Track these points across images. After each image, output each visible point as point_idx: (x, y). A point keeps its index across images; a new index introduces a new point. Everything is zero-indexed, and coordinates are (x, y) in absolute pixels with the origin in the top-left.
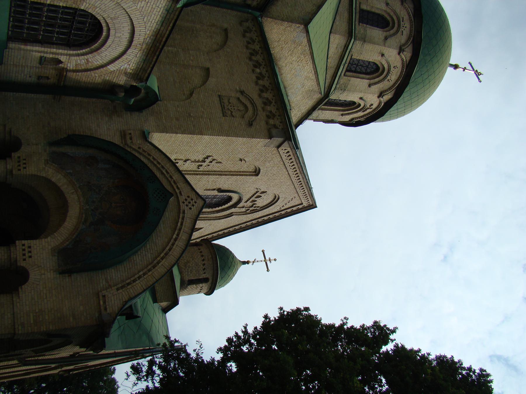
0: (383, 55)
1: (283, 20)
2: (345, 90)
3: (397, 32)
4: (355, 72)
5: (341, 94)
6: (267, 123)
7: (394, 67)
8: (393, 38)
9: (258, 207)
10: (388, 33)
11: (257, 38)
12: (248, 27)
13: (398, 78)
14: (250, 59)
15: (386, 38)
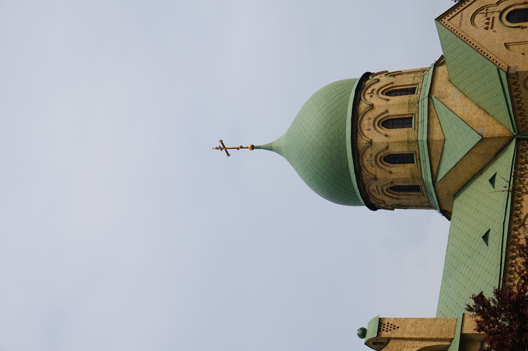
0: (386, 136)
1: (499, 137)
2: (409, 104)
3: (377, 156)
4: (403, 118)
5: (410, 100)
6: (518, 79)
7: (370, 130)
8: (379, 150)
9: (480, 13)
10: (386, 152)
11: (518, 123)
12: (523, 127)
13: (361, 122)
14: (524, 110)
15: (387, 148)
